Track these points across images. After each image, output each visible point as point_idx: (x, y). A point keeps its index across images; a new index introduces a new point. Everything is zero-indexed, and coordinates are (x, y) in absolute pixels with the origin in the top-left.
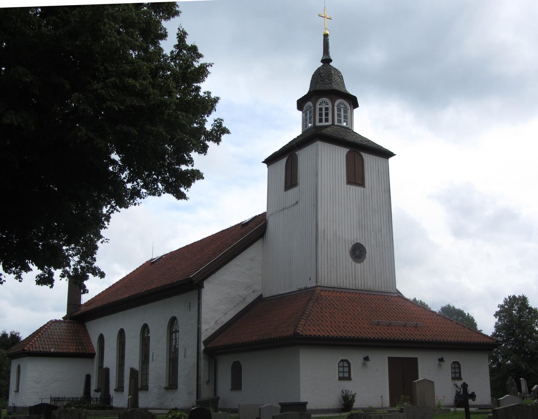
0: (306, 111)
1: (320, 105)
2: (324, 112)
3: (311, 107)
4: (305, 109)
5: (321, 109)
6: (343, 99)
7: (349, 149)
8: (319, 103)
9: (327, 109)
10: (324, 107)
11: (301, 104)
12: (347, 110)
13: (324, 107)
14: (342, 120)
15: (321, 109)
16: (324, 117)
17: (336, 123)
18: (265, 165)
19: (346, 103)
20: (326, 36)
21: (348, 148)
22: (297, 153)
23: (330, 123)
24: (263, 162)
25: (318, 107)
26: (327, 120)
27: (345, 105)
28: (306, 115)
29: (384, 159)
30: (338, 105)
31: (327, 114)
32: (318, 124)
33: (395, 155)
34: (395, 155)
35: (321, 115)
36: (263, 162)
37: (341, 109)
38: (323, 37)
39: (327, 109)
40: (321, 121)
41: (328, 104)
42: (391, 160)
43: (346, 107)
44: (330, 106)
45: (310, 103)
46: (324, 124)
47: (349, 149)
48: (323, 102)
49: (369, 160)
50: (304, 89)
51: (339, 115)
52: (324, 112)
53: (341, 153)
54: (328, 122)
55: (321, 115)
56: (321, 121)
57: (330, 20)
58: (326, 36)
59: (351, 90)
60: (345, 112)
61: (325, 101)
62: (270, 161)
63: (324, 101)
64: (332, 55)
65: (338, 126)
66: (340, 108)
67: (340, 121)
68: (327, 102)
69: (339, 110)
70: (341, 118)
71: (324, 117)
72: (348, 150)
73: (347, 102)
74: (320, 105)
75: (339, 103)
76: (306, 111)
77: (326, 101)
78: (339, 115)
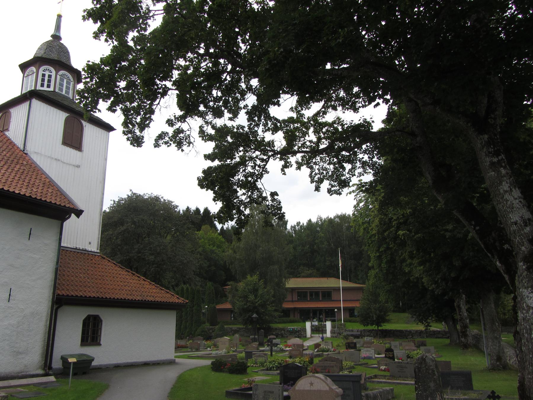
0: (28, 75)
2: (46, 78)
3: (34, 73)
5: (44, 75)
7: (69, 115)
9: (50, 76)
10: (47, 73)
13: (47, 73)
15: (44, 75)
16: (46, 83)
20: (59, 17)
21: (68, 113)
23: (51, 89)
25: (41, 72)
26: (49, 86)
27: (68, 77)
30: (61, 75)
32: (39, 88)
33: (115, 129)
34: (115, 129)
35: (43, 80)
38: (56, 17)
39: (50, 76)
40: (42, 85)
41: (51, 72)
42: (111, 133)
45: (34, 69)
46: (45, 88)
47: (69, 115)
48: (47, 69)
50: (29, 56)
52: (46, 78)
53: (60, 117)
55: (43, 80)
56: (42, 85)
58: (59, 17)
63: (48, 68)
64: (63, 34)
67: (61, 89)
68: (50, 70)
69: (62, 80)
71: (46, 83)
72: (67, 115)
74: (43, 71)
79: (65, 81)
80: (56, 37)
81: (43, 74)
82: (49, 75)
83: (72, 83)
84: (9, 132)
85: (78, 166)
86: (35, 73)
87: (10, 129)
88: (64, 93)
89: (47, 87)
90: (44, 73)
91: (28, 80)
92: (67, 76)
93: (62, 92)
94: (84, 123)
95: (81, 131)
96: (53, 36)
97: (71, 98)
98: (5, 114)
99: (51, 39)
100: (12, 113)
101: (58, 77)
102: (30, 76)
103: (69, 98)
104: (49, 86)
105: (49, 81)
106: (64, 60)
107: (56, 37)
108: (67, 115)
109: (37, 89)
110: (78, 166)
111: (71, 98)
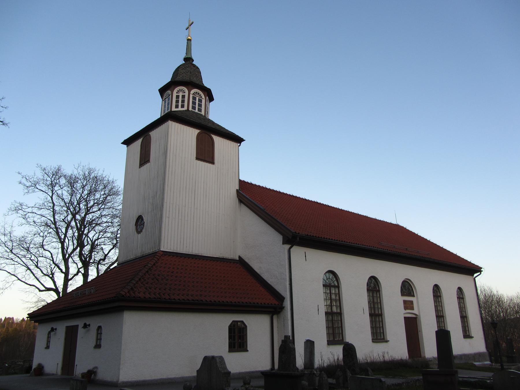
0: (165, 99)
1: (177, 93)
2: (180, 99)
3: (170, 95)
4: (164, 98)
6: (199, 89)
8: (176, 91)
9: (183, 97)
10: (181, 94)
12: (202, 100)
14: (196, 107)
15: (178, 97)
16: (180, 104)
17: (190, 109)
18: (125, 146)
19: (203, 94)
21: (199, 130)
23: (185, 108)
24: (122, 143)
26: (183, 106)
27: (200, 95)
28: (165, 102)
30: (193, 93)
31: (183, 101)
32: (174, 109)
33: (245, 140)
34: (245, 140)
36: (121, 143)
37: (196, 98)
39: (183, 97)
40: (177, 106)
41: (185, 93)
43: (201, 97)
44: (186, 94)
45: (169, 92)
46: (180, 109)
47: (200, 131)
51: (194, 103)
52: (180, 99)
53: (192, 133)
54: (184, 108)
55: (177, 102)
56: (177, 106)
57: (193, 24)
59: (206, 83)
60: (200, 101)
61: (183, 89)
62: (128, 142)
65: (191, 110)
66: (195, 97)
67: (194, 108)
69: (194, 98)
70: (196, 105)
71: (180, 104)
72: (198, 131)
73: (201, 91)
75: (195, 92)
76: (165, 99)
77: (183, 89)
78: (194, 103)
79: (197, 98)
80: (188, 60)
81: (176, 95)
82: (182, 96)
83: (203, 101)
86: (171, 95)
88: (197, 111)
89: (181, 108)
91: (165, 102)
92: (199, 94)
93: (195, 110)
95: (212, 145)
96: (186, 59)
97: (204, 115)
98: (145, 137)
99: (184, 62)
101: (191, 96)
102: (167, 99)
103: (201, 115)
104: (183, 106)
106: (195, 80)
107: (188, 60)
108: (200, 131)
109: (173, 110)
111: (204, 115)
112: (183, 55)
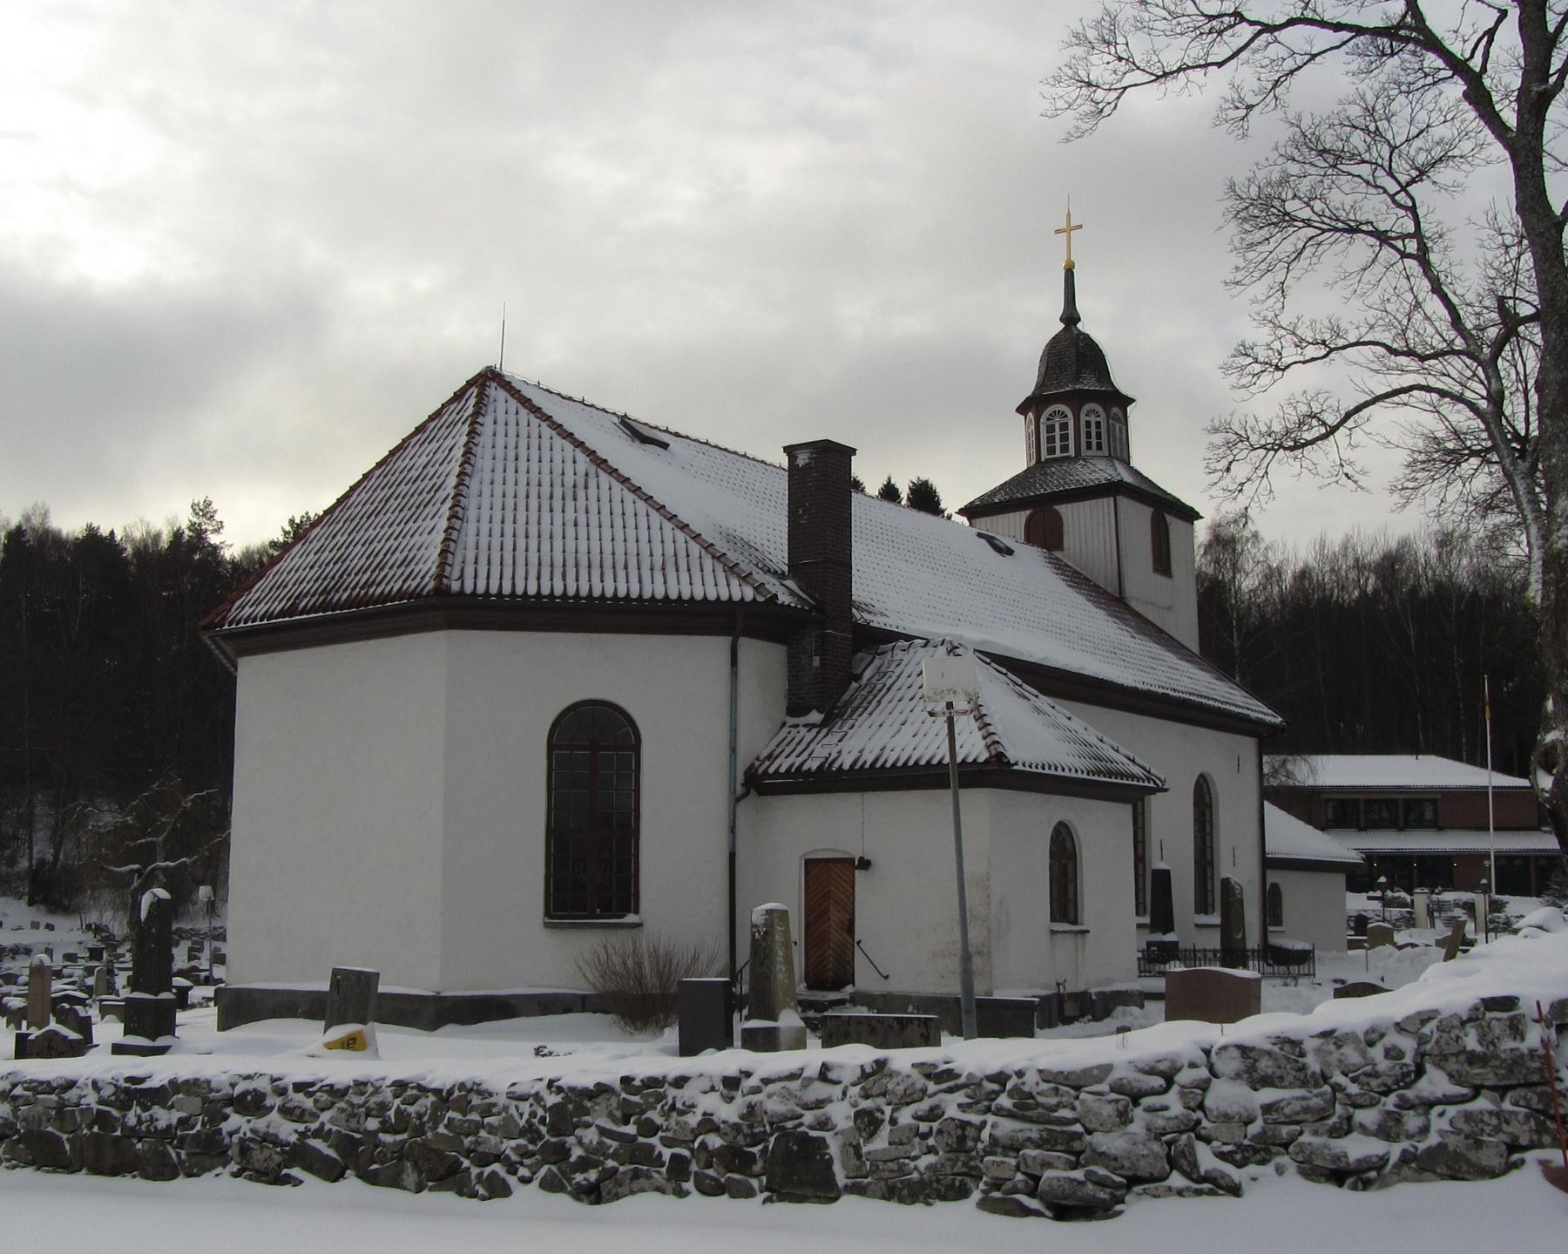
5: (1088, 424)
9: (1098, 424)
10: (1093, 419)
11: (1031, 406)
13: (1093, 419)
15: (1088, 424)
22: (1057, 507)
25: (1083, 419)
29: (1189, 525)
33: (1202, 517)
34: (1202, 517)
35: (1089, 435)
39: (1098, 424)
44: (1102, 419)
49: (1175, 525)
55: (1089, 435)
74: (1087, 415)
80: (1070, 317)
84: (1066, 552)
85: (1169, 608)
87: (1065, 546)
90: (1088, 418)
94: (1169, 518)
100: (1064, 517)
105: (1099, 435)
107: (1070, 317)
110: (1169, 608)
112: (1060, 308)
